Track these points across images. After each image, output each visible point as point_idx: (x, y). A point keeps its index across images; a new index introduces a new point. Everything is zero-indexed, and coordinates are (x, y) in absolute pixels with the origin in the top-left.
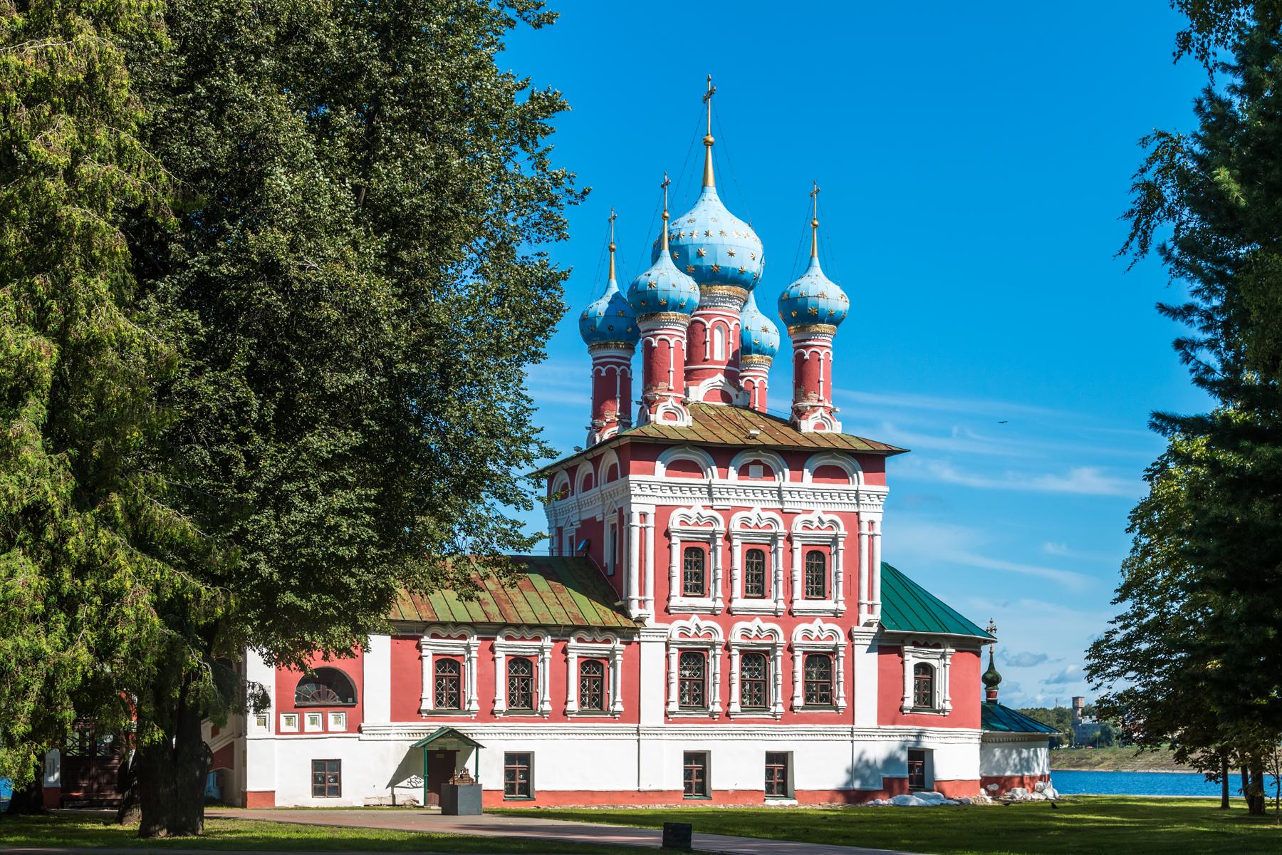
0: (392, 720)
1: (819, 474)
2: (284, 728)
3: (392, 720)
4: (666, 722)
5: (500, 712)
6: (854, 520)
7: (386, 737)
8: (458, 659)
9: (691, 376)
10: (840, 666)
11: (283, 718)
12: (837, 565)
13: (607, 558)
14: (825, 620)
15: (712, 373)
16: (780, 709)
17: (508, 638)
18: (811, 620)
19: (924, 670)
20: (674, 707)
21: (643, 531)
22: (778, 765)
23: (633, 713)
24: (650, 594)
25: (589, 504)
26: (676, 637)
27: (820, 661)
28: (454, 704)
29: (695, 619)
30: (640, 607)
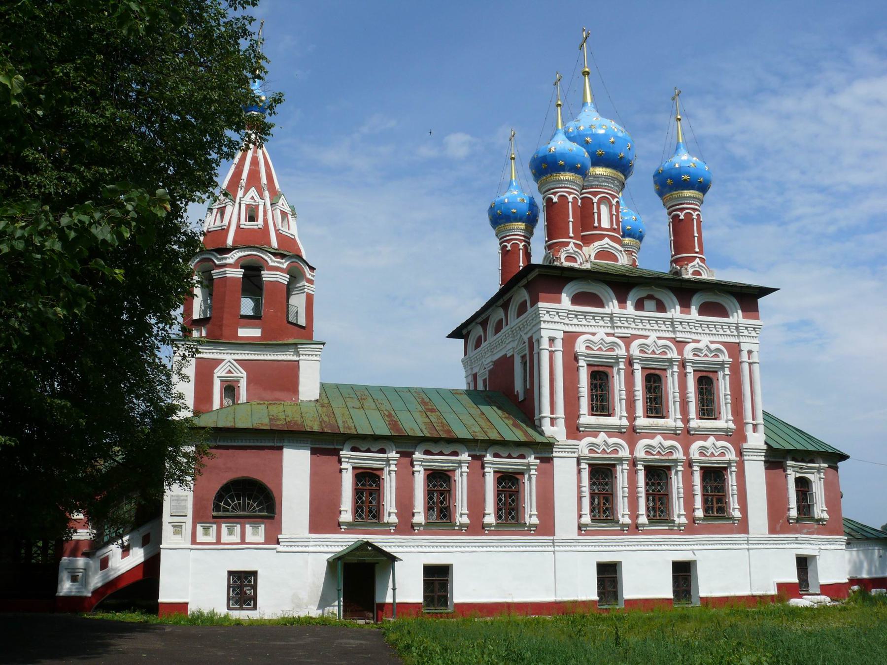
1: (705, 309)
2: (200, 538)
4: (579, 534)
6: (734, 349)
7: (304, 549)
8: (377, 473)
10: (732, 480)
11: (199, 528)
12: (723, 387)
13: (518, 387)
14: (718, 438)
15: (601, 237)
16: (683, 520)
17: (427, 452)
18: (705, 438)
19: (803, 485)
20: (587, 519)
22: (683, 572)
23: (546, 527)
24: (560, 412)
25: (501, 345)
26: (586, 452)
28: (374, 517)
29: (602, 436)
30: (552, 424)
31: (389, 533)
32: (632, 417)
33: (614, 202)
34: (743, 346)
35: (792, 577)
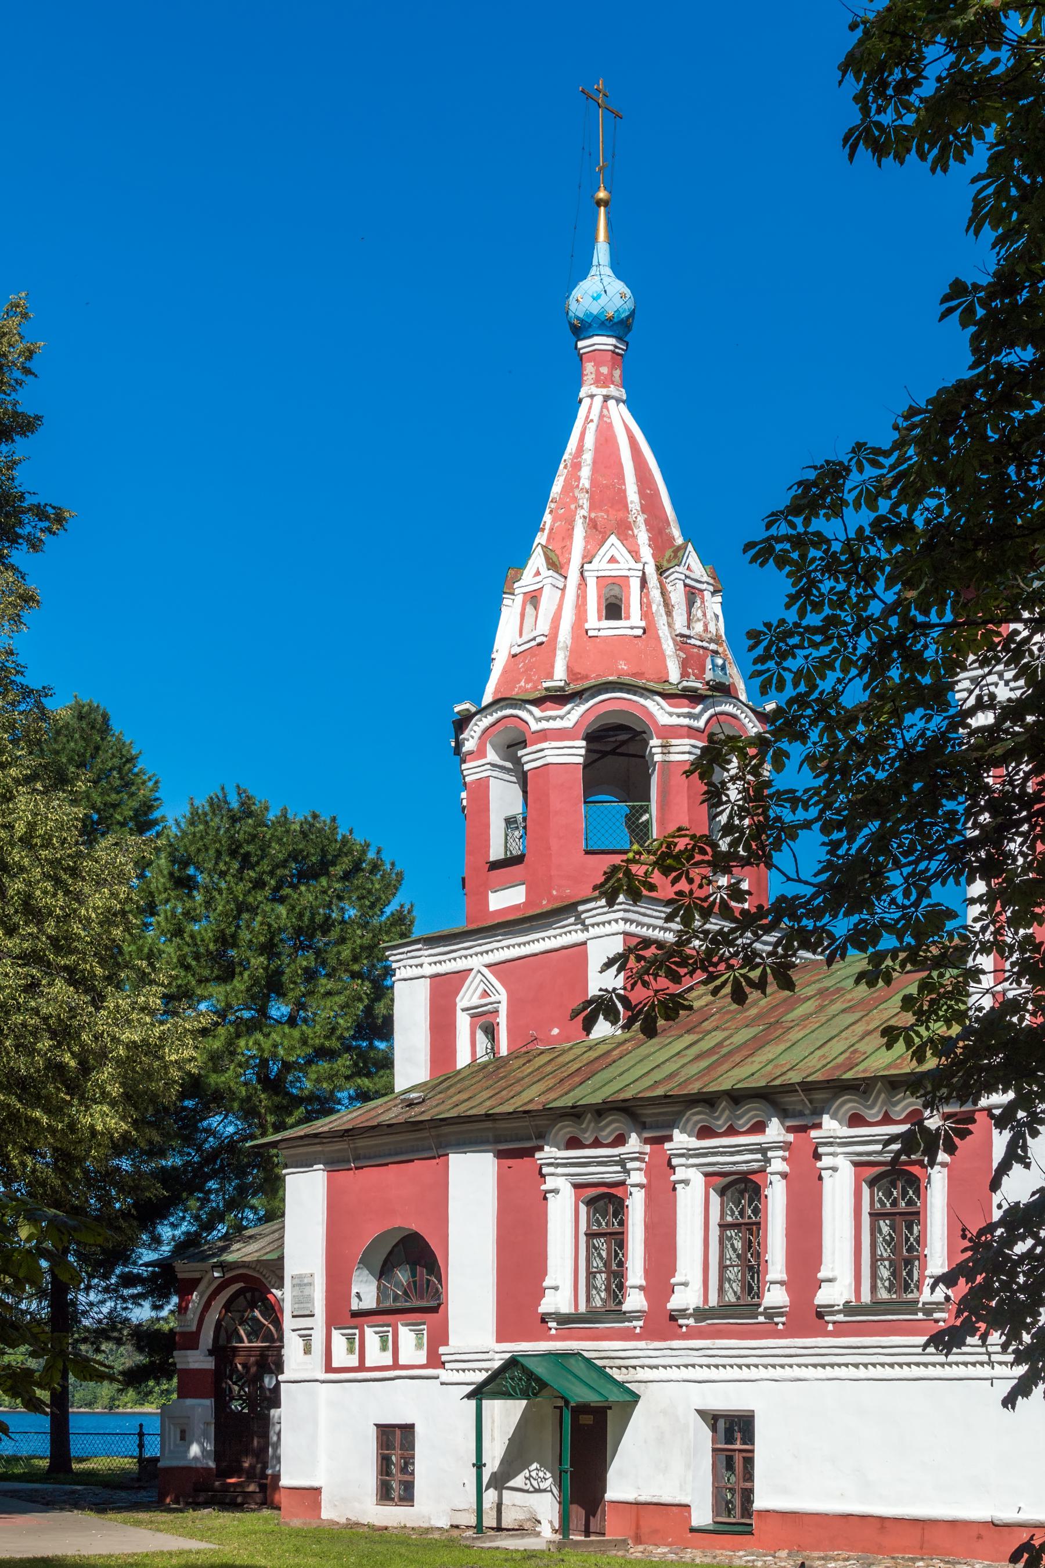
0: (500, 1339)
2: (342, 1357)
3: (500, 1339)
5: (683, 1313)
8: (618, 1192)
11: (339, 1340)
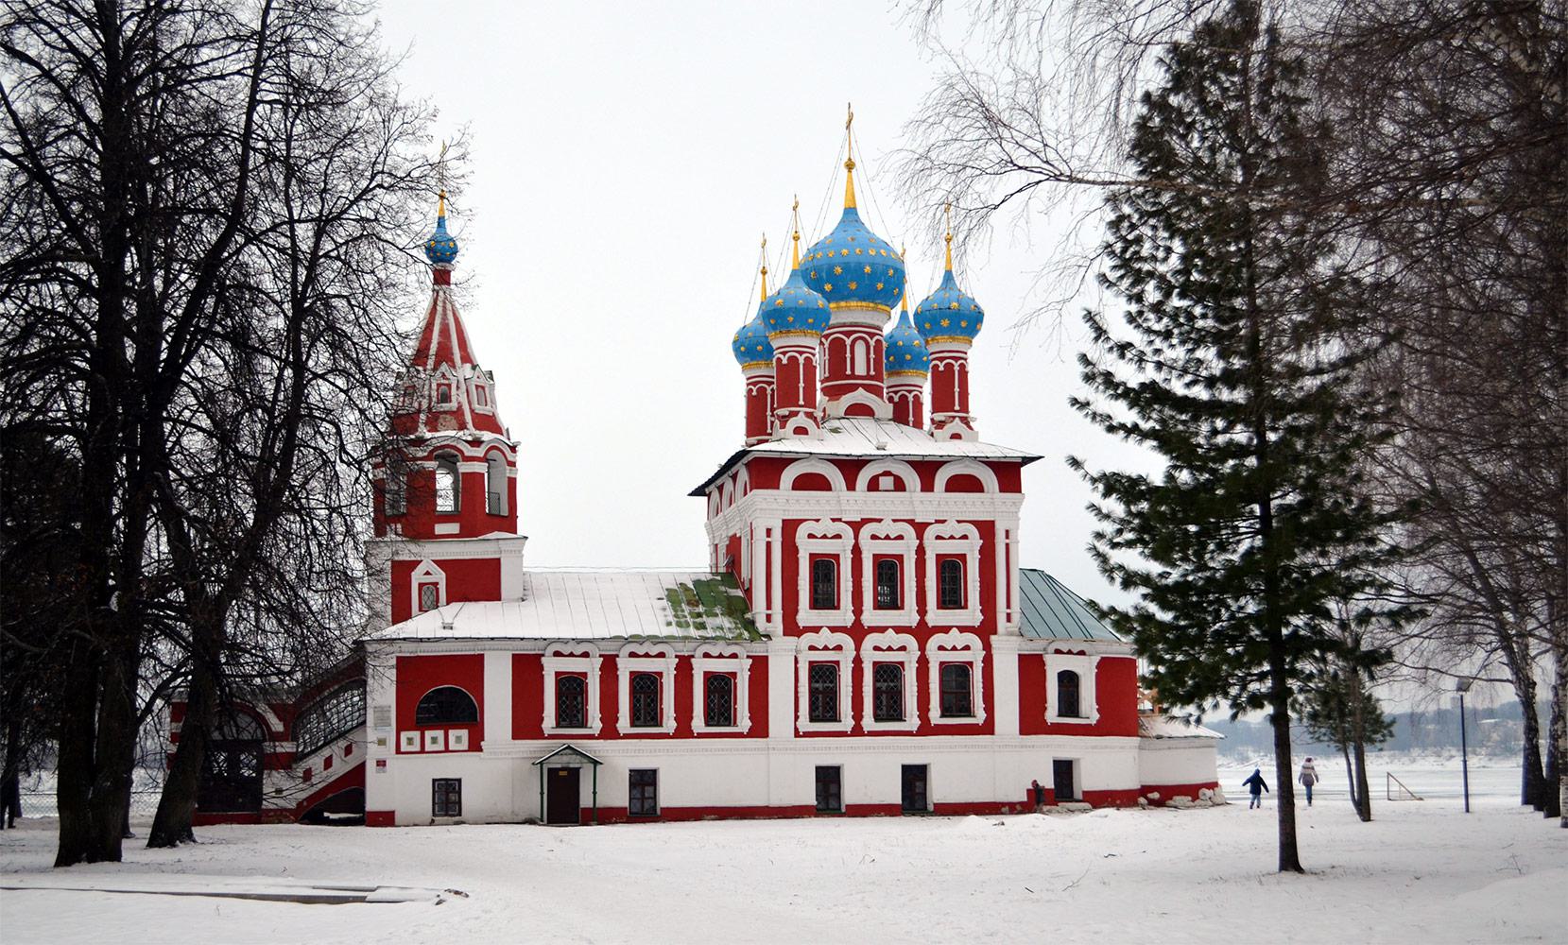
2: (404, 747)
4: (797, 734)
6: (987, 529)
9: (833, 393)
15: (853, 388)
18: (946, 630)
20: (805, 724)
21: (769, 545)
22: (914, 777)
23: (760, 728)
27: (956, 676)
29: (825, 630)
31: (591, 737)
32: (858, 611)
33: (872, 343)
34: (998, 526)
35: (1048, 782)
